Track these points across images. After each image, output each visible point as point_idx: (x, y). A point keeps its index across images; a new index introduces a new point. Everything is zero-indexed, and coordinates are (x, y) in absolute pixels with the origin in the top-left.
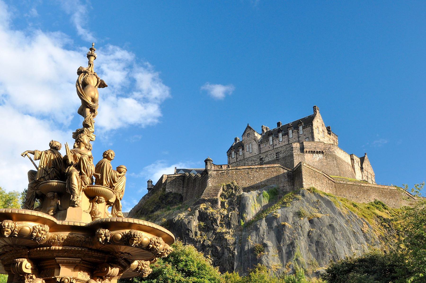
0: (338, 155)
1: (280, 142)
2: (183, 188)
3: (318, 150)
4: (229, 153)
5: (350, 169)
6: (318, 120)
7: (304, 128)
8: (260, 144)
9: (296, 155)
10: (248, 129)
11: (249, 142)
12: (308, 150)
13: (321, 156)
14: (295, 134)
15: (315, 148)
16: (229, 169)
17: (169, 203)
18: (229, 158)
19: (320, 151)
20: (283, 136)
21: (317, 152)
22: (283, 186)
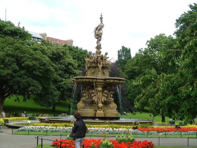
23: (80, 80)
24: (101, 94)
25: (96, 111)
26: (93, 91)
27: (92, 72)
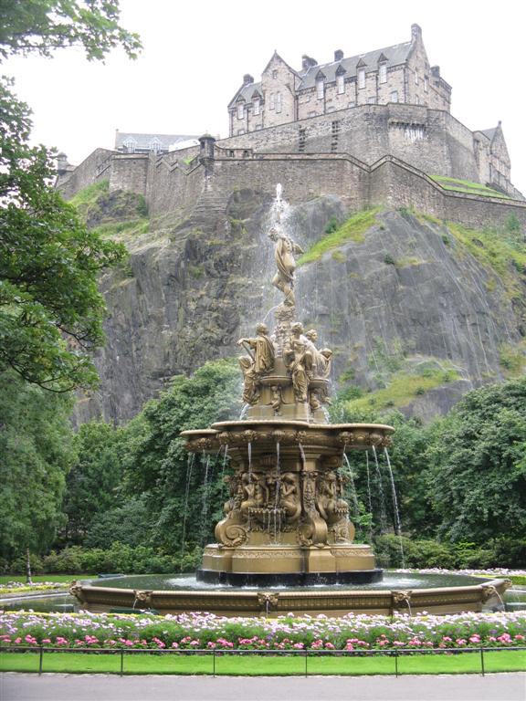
0: (451, 134)
1: (339, 96)
2: (145, 183)
3: (415, 122)
4: (233, 111)
5: (471, 160)
6: (420, 55)
7: (390, 70)
8: (298, 94)
9: (372, 130)
10: (276, 62)
11: (276, 90)
12: (396, 121)
13: (419, 134)
14: (371, 82)
15: (410, 118)
16: (247, 158)
17: (117, 213)
18: (232, 120)
19: (418, 125)
20: (345, 83)
21: (414, 127)
22: (350, 199)
23: (248, 432)
24: (313, 484)
25: (304, 550)
26: (291, 476)
27: (275, 403)
